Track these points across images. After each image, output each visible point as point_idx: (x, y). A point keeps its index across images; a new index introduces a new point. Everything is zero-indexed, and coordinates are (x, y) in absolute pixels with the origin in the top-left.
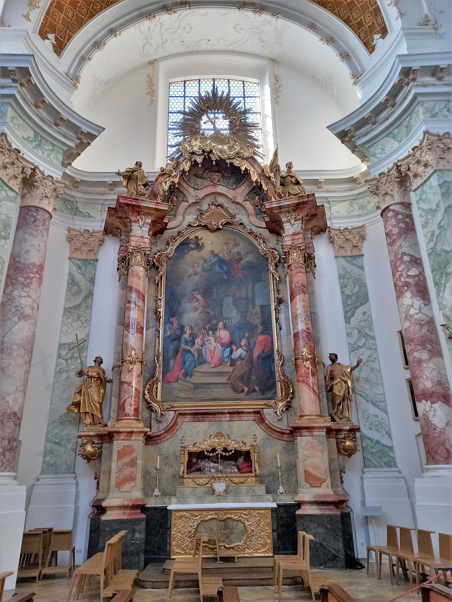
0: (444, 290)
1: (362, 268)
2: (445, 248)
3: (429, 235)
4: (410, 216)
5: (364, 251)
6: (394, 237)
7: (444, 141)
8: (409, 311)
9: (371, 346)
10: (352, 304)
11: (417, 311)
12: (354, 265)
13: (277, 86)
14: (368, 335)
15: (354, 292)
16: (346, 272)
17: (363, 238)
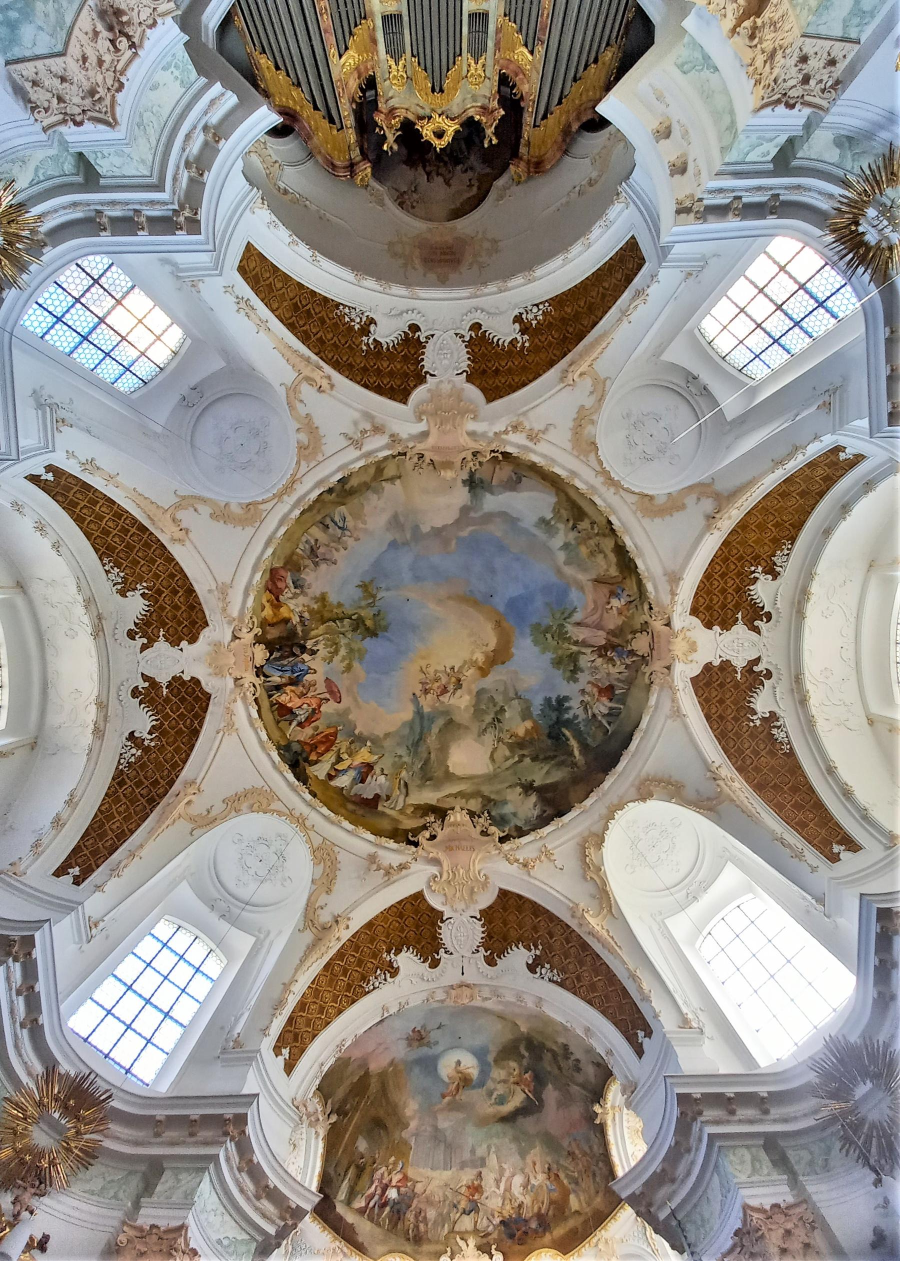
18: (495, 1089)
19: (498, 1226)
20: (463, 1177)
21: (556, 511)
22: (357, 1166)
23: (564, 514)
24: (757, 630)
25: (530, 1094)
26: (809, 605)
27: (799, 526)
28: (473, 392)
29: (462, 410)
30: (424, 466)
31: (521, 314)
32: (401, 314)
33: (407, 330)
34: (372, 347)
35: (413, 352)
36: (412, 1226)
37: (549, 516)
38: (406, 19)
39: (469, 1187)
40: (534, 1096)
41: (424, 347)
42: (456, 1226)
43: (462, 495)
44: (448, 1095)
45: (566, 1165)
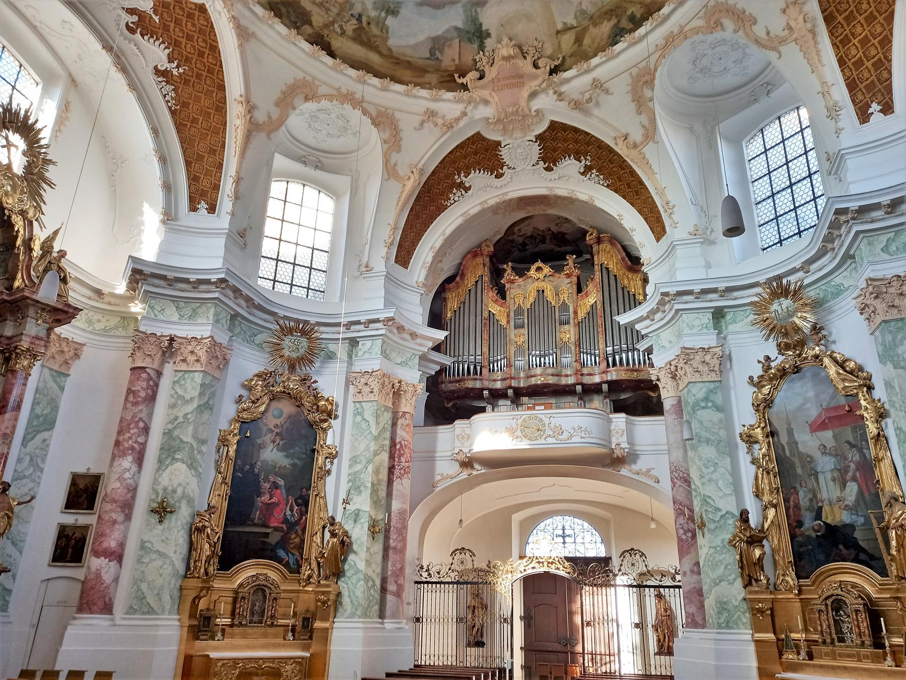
0: (164, 470)
1: (62, 389)
2: (181, 436)
3: (172, 417)
4: (157, 385)
5: (71, 372)
6: (139, 399)
7: (217, 348)
8: (124, 474)
9: (36, 479)
10: (37, 426)
11: (131, 476)
12: (56, 382)
13: (64, 115)
14: (38, 466)
15: (44, 412)
16: (46, 387)
17: (77, 356)
21: (384, 29)
23: (375, 30)
24: (131, 11)
26: (110, 60)
27: (180, 127)
28: (492, 135)
29: (503, 122)
30: (532, 51)
31: (466, 192)
32: (559, 178)
33: (555, 168)
34: (582, 158)
35: (549, 154)
37: (390, 21)
38: (557, 324)
41: (539, 158)
43: (489, 18)
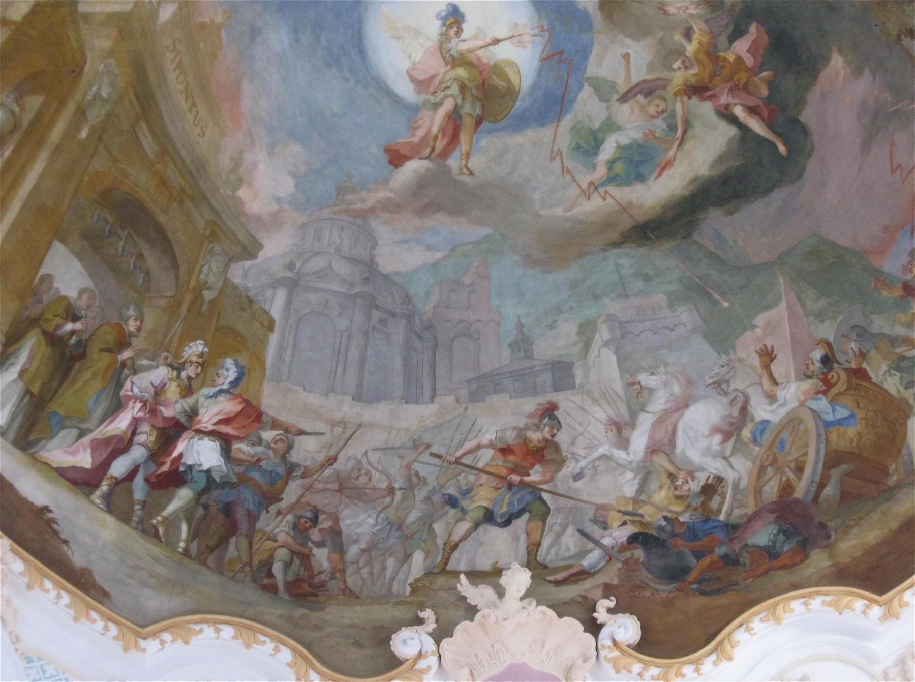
18: (610, 126)
19: (622, 549)
20: (483, 421)
22: (53, 339)
25: (756, 126)
36: (282, 553)
39: (505, 451)
40: (769, 123)
42: (456, 555)
44: (415, 151)
45: (900, 331)
